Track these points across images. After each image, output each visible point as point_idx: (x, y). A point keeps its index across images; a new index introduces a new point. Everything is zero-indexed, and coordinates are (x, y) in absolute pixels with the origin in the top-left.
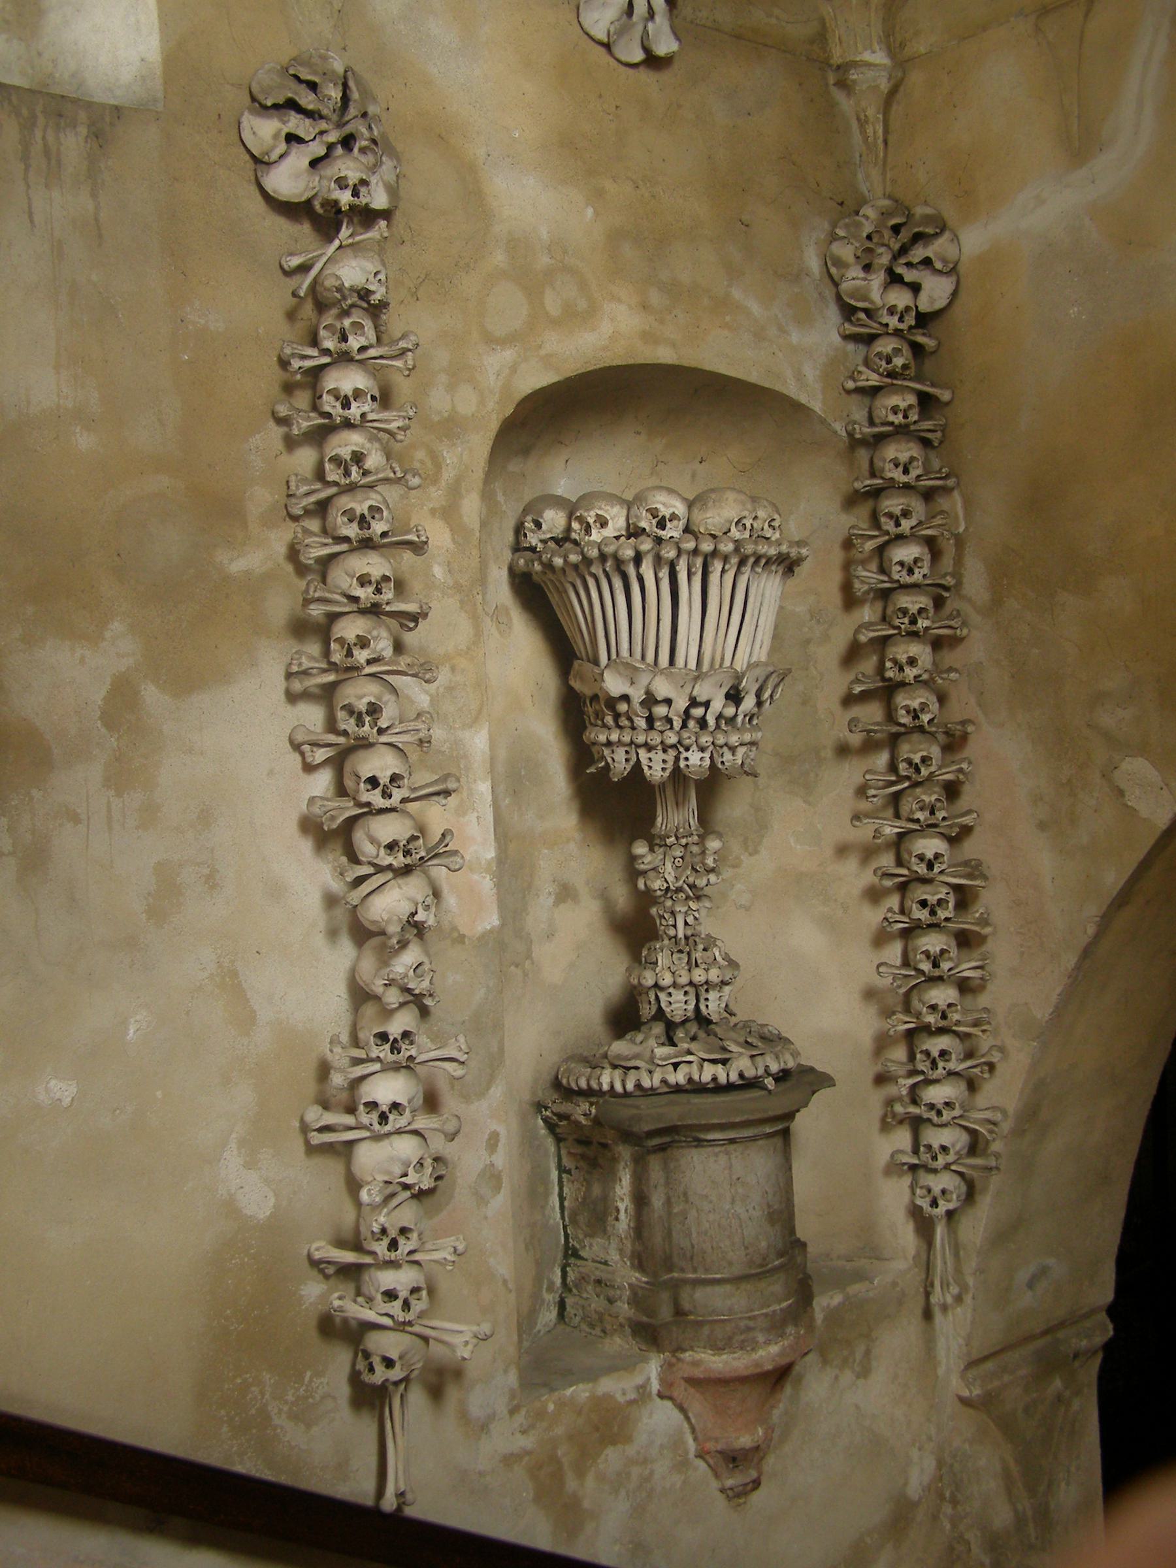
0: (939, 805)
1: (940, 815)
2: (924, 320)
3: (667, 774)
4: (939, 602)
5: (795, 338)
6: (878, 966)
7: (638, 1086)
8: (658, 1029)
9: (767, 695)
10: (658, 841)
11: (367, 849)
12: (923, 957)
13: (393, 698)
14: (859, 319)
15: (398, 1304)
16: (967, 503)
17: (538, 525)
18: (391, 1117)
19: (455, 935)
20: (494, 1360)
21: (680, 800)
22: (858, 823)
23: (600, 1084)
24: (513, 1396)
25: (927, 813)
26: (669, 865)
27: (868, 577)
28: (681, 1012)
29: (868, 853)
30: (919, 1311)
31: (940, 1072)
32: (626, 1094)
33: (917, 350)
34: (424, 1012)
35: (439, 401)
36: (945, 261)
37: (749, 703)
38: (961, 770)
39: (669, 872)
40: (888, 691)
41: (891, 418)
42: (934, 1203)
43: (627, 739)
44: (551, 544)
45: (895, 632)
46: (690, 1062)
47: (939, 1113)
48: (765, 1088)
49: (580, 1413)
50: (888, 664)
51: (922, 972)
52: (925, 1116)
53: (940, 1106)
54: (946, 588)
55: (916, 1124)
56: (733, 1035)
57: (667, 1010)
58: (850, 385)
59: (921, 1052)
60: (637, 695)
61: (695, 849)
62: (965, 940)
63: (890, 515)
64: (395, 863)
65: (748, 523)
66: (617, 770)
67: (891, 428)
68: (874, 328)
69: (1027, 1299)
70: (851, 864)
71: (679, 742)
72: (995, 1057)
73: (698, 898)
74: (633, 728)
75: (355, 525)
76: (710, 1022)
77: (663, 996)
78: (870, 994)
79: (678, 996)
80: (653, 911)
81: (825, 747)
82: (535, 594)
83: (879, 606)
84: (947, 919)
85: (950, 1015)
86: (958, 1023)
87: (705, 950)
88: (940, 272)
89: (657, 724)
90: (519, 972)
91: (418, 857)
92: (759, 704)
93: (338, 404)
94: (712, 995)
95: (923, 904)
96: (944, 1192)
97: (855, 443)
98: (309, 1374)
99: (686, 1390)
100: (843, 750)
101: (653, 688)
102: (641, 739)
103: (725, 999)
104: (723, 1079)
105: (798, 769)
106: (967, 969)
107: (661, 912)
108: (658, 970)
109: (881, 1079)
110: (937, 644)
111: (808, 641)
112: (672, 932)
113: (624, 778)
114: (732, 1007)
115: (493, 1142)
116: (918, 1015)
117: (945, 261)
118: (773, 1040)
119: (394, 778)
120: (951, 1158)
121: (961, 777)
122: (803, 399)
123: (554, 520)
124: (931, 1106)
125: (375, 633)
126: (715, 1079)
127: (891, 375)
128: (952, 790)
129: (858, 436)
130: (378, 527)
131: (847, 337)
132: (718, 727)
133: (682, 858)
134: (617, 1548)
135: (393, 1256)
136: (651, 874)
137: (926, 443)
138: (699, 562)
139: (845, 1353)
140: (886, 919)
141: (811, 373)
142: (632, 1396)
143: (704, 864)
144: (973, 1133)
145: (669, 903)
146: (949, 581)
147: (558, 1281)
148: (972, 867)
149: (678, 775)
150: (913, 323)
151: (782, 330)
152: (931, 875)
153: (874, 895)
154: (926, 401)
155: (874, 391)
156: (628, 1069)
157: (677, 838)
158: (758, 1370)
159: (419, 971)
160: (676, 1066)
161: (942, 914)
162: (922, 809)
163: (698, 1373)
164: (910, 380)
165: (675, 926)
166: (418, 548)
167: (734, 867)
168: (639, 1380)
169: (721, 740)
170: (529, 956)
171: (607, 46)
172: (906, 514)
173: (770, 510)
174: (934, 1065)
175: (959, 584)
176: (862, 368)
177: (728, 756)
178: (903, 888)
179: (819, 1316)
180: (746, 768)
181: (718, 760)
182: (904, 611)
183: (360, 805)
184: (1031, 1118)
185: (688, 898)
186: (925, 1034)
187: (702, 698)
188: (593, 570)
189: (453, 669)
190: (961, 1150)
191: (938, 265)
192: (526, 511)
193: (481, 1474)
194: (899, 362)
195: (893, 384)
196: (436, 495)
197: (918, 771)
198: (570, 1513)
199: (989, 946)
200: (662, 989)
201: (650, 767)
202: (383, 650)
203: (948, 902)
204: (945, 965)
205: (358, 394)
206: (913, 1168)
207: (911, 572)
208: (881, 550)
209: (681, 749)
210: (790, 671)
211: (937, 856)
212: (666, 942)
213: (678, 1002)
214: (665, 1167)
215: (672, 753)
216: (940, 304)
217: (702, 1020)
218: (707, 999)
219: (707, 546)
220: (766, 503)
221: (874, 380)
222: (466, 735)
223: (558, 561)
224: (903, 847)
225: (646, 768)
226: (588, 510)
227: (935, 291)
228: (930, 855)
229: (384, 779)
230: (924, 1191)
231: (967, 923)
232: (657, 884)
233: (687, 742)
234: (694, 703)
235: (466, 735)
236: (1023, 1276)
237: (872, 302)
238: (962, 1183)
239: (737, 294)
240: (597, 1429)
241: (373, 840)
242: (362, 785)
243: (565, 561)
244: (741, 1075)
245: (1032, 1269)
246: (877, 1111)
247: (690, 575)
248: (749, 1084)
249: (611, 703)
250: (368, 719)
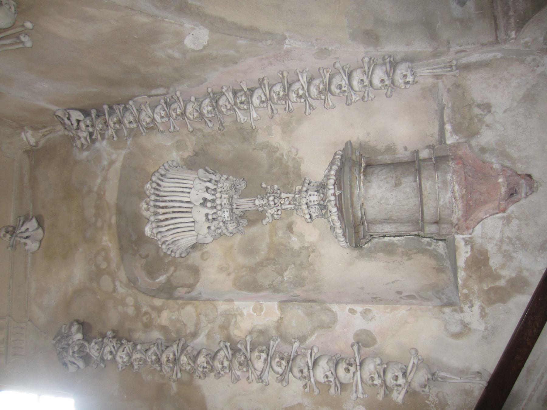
19: (280, 321)
20: (438, 318)
24: (455, 310)
35: (131, 311)
49: (471, 277)
90: (312, 255)
98: (427, 402)
99: (472, 220)
111: (204, 136)
115: (352, 311)
117: (65, 114)
134: (539, 259)
139: (476, 120)
142: (469, 247)
147: (428, 239)
151: (103, 169)
167: (283, 156)
168: (463, 243)
170: (307, 248)
171: (41, 241)
187: (204, 218)
189: (201, 314)
191: (67, 116)
193: (486, 329)
196: (154, 315)
198: (517, 284)
216: (80, 113)
218: (314, 201)
222: (220, 311)
235: (220, 311)
239: (96, 189)
240: (480, 268)
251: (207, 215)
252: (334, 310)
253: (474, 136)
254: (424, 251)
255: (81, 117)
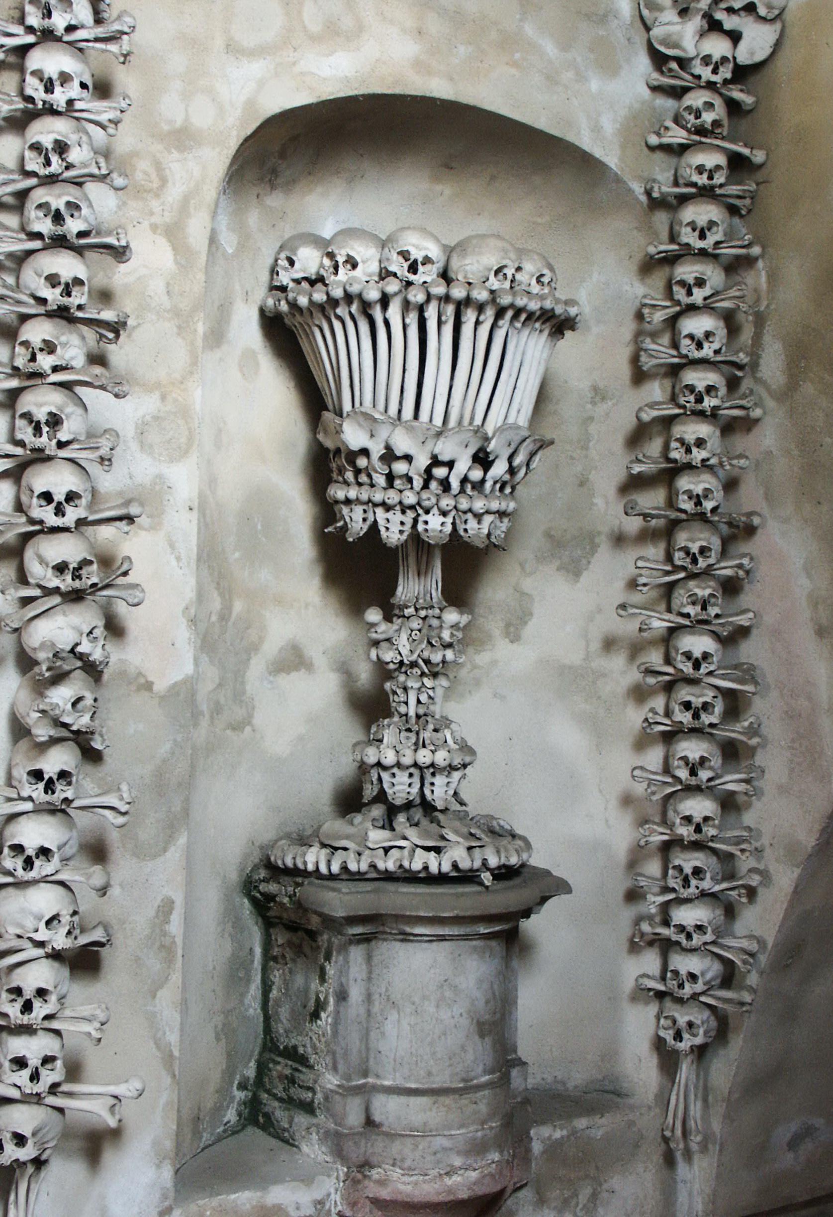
0: (713, 600)
1: (713, 611)
2: (742, 73)
3: (404, 537)
4: (733, 384)
5: (594, 85)
6: (635, 769)
7: (345, 868)
8: (377, 811)
9: (518, 460)
10: (397, 612)
11: (36, 570)
12: (682, 763)
13: (80, 411)
14: (670, 70)
15: (26, 1073)
16: (773, 277)
17: (292, 263)
18: (37, 863)
19: (142, 681)
21: (423, 567)
22: (622, 613)
23: (305, 863)
25: (698, 608)
26: (404, 636)
27: (660, 352)
28: (404, 795)
29: (636, 650)
30: (657, 1158)
31: (692, 890)
32: (331, 877)
33: (733, 107)
34: (92, 756)
36: (770, 7)
37: (499, 469)
38: (740, 566)
39: (403, 643)
40: (670, 473)
41: (695, 178)
42: (678, 1036)
43: (364, 497)
44: (305, 285)
45: (681, 411)
46: (401, 848)
47: (689, 937)
48: (481, 884)
50: (674, 444)
51: (678, 780)
52: (674, 938)
53: (690, 929)
54: (740, 367)
55: (666, 946)
56: (457, 824)
57: (389, 791)
58: (654, 140)
59: (674, 867)
60: (377, 450)
61: (435, 623)
62: (732, 752)
63: (682, 283)
64: (62, 587)
65: (509, 272)
66: (354, 531)
67: (693, 190)
68: (686, 80)
69: (787, 1160)
70: (618, 661)
71: (419, 504)
72: (755, 880)
73: (435, 675)
74: (372, 486)
75: (49, 221)
76: (435, 809)
77: (385, 776)
78: (627, 800)
79: (402, 777)
80: (388, 686)
81: (599, 533)
82: (285, 334)
83: (668, 383)
84: (712, 725)
85: (705, 829)
86: (713, 838)
87: (436, 730)
88: (764, 19)
89: (397, 483)
91: (90, 583)
92: (512, 471)
93: (41, 88)
94: (440, 780)
95: (687, 705)
96: (690, 1025)
97: (656, 203)
100: (619, 540)
101: (392, 442)
102: (378, 497)
103: (453, 786)
104: (434, 869)
105: (570, 551)
106: (731, 782)
107: (394, 688)
108: (382, 747)
109: (633, 895)
110: (729, 428)
112: (403, 709)
113: (360, 538)
114: (463, 796)
116: (671, 827)
118: (499, 834)
119: (71, 497)
120: (699, 987)
121: (741, 573)
122: (597, 152)
123: (309, 260)
124: (681, 928)
125: (63, 339)
126: (426, 868)
127: (701, 131)
128: (731, 587)
129: (655, 195)
130: (73, 226)
131: (655, 89)
132: (462, 491)
133: (420, 630)
135: (25, 1019)
136: (384, 645)
137: (733, 210)
138: (450, 309)
140: (646, 720)
141: (609, 125)
143: (440, 638)
144: (728, 964)
145: (402, 678)
146: (742, 358)
148: (744, 671)
149: (417, 541)
150: (729, 76)
152: (697, 675)
153: (639, 694)
154: (738, 164)
155: (682, 149)
156: (336, 849)
157: (417, 610)
158: (451, 1197)
159: (80, 706)
160: (387, 850)
161: (706, 719)
162: (694, 603)
163: (384, 1194)
164: (723, 138)
165: (406, 703)
166: (120, 253)
168: (318, 1195)
169: (464, 504)
172: (700, 282)
173: (539, 265)
174: (686, 883)
175: (754, 365)
176: (669, 123)
177: (472, 524)
178: (669, 688)
179: (537, 1147)
180: (493, 539)
181: (461, 528)
182: (691, 389)
183: (32, 521)
184: (790, 953)
185: (423, 674)
186: (678, 849)
187: (445, 457)
188: (339, 311)
189: (163, 398)
190: (713, 979)
191: (762, 11)
192: (282, 248)
194: (708, 117)
195: (701, 143)
197: (695, 561)
199: (760, 759)
200: (385, 768)
201: (387, 529)
202: (72, 358)
203: (714, 706)
204: (704, 775)
205: (65, 78)
206: (660, 995)
207: (700, 346)
208: (672, 322)
209: (420, 511)
210: (552, 443)
211: (706, 656)
212: (396, 719)
213: (401, 784)
214: (369, 958)
215: (410, 514)
216: (759, 57)
217: (428, 807)
218: (432, 784)
219: (458, 293)
220: (536, 257)
221: (677, 136)
223: (303, 301)
224: (671, 643)
225: (383, 530)
226: (340, 248)
227: (756, 42)
228: (697, 654)
229: (59, 497)
230: (669, 1022)
231: (735, 731)
232: (389, 656)
233: (426, 504)
234: (436, 462)
236: (784, 1133)
237: (684, 50)
238: (712, 1018)
239: (529, 30)
241: (42, 561)
242: (35, 500)
243: (310, 301)
244: (455, 866)
245: (794, 1127)
246: (625, 929)
247: (440, 323)
248: (466, 877)
249: (352, 456)
250: (45, 429)
251: (450, 464)
252: (168, 854)
253: (538, 1193)
254: (229, 1072)
255: (745, 54)
